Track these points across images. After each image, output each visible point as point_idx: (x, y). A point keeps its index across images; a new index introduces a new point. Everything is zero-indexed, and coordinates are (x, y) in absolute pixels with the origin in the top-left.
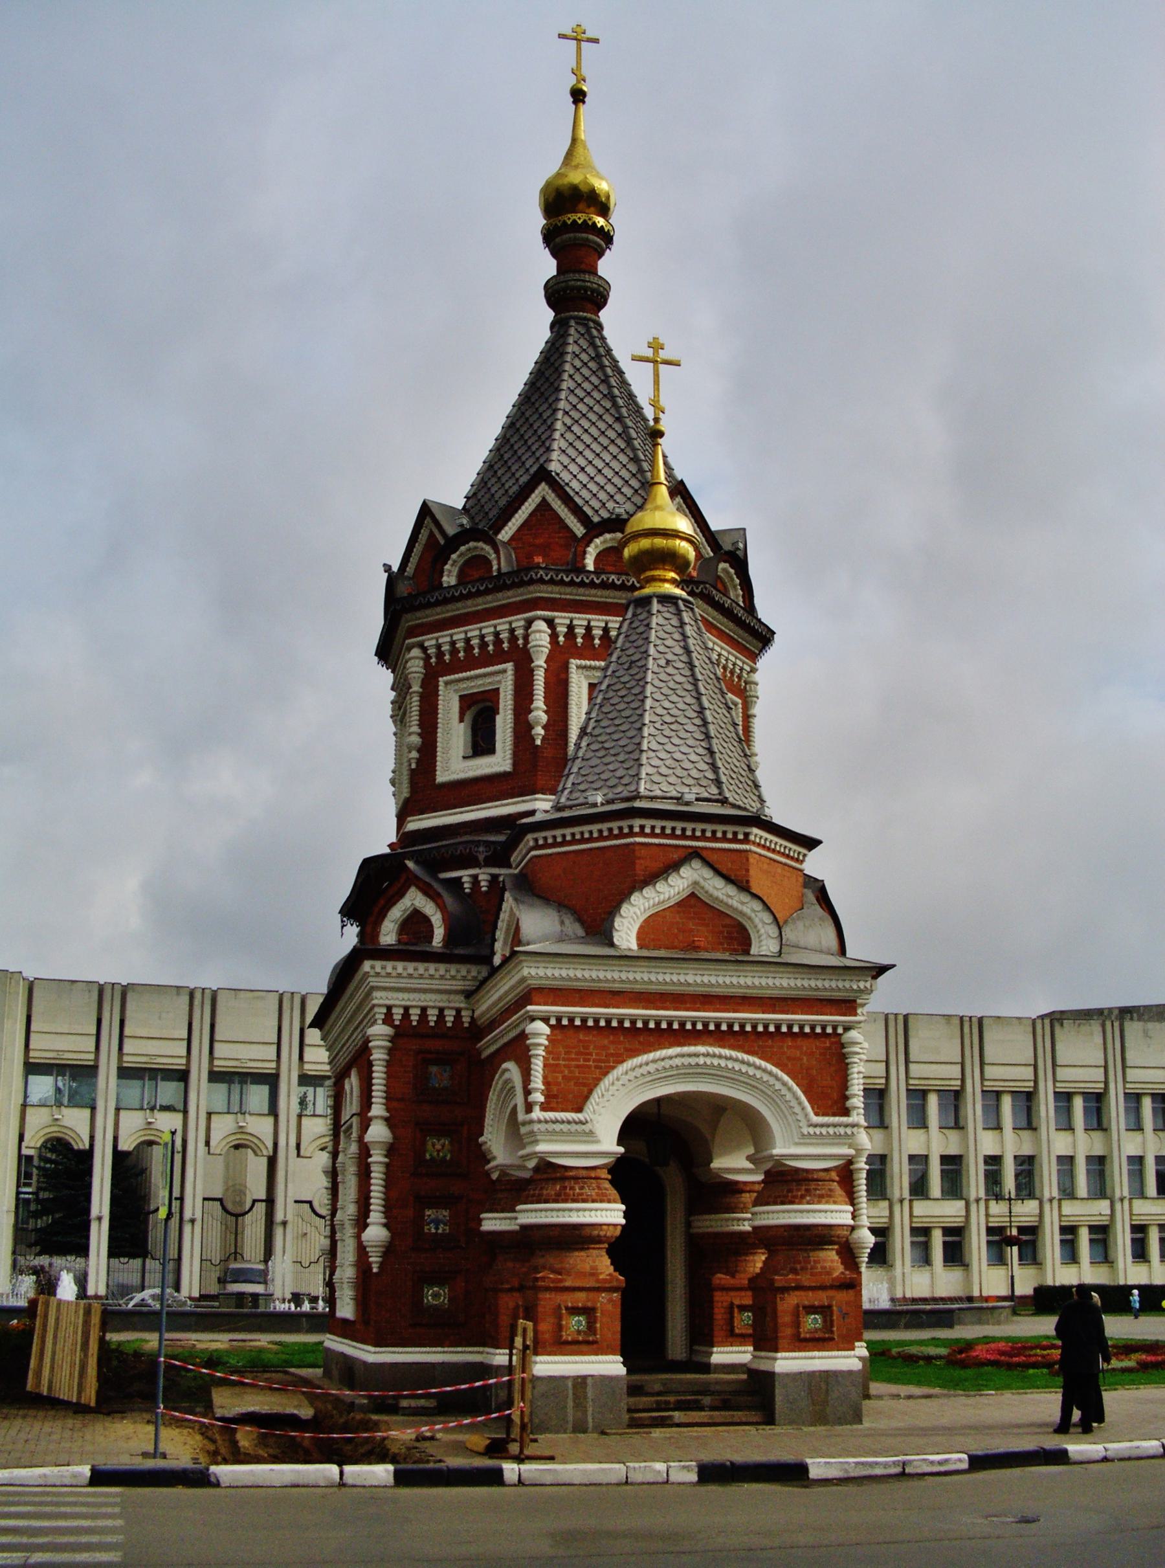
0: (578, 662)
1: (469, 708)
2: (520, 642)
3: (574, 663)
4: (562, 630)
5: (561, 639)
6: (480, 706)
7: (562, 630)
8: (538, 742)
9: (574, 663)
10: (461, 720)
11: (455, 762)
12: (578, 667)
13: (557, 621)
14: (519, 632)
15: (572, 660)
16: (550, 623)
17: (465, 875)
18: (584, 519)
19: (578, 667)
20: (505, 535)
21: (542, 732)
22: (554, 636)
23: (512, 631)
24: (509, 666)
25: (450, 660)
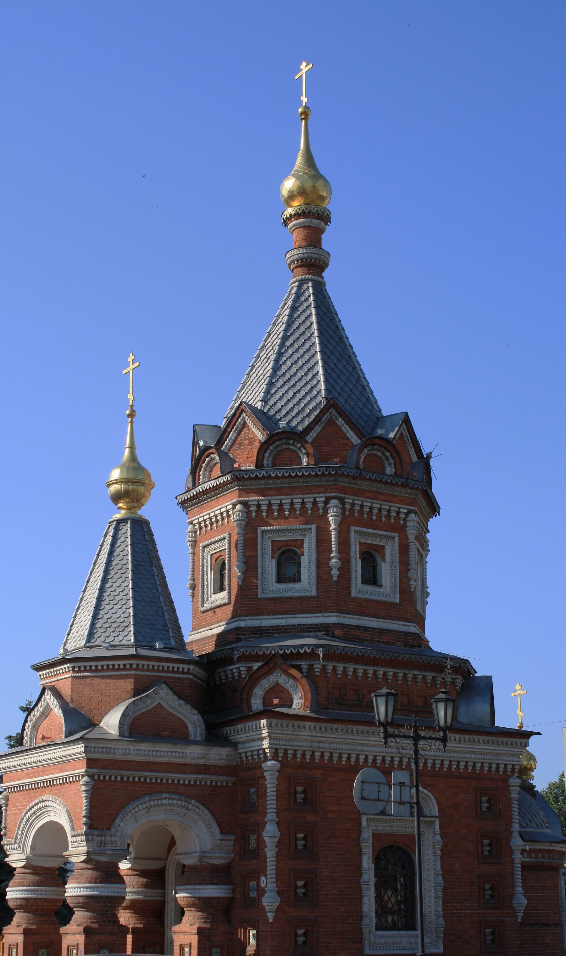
0: (358, 529)
1: (279, 549)
2: (321, 511)
3: (353, 528)
4: (348, 506)
5: (347, 513)
6: (283, 549)
7: (348, 506)
8: (335, 579)
9: (353, 528)
10: (273, 558)
11: (270, 586)
12: (356, 532)
13: (346, 500)
14: (321, 505)
15: (352, 527)
16: (342, 501)
17: (304, 665)
18: (360, 434)
19: (356, 532)
20: (309, 438)
21: (338, 572)
22: (343, 509)
23: (315, 503)
24: (314, 527)
25: (256, 517)
